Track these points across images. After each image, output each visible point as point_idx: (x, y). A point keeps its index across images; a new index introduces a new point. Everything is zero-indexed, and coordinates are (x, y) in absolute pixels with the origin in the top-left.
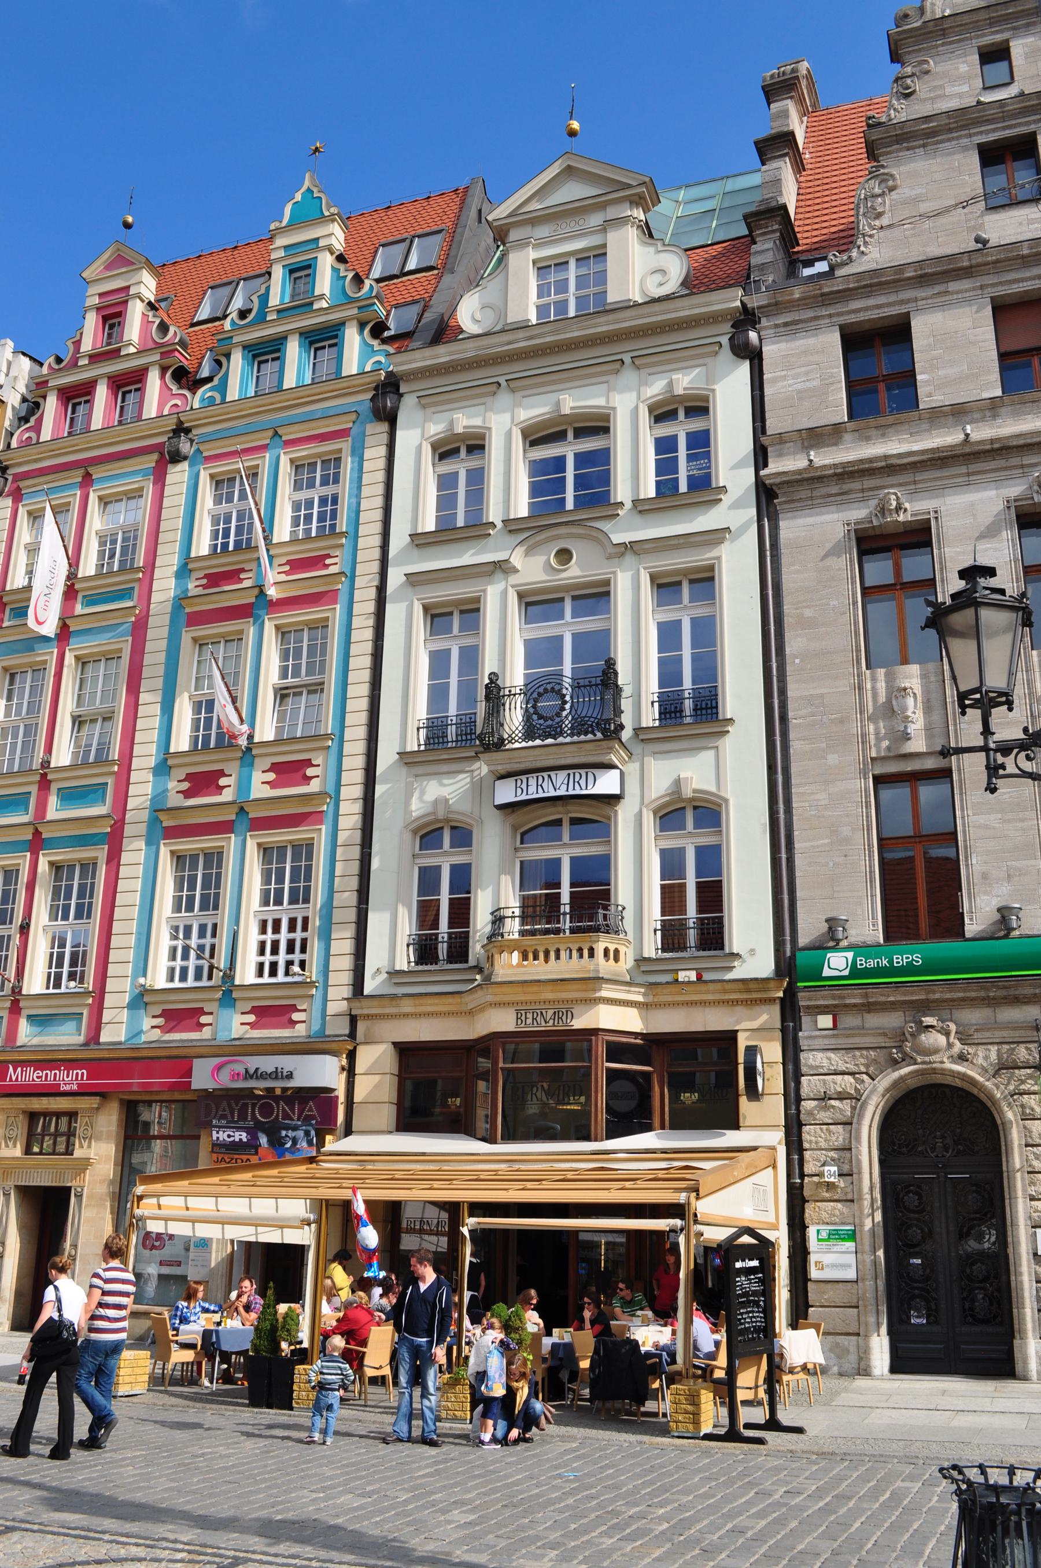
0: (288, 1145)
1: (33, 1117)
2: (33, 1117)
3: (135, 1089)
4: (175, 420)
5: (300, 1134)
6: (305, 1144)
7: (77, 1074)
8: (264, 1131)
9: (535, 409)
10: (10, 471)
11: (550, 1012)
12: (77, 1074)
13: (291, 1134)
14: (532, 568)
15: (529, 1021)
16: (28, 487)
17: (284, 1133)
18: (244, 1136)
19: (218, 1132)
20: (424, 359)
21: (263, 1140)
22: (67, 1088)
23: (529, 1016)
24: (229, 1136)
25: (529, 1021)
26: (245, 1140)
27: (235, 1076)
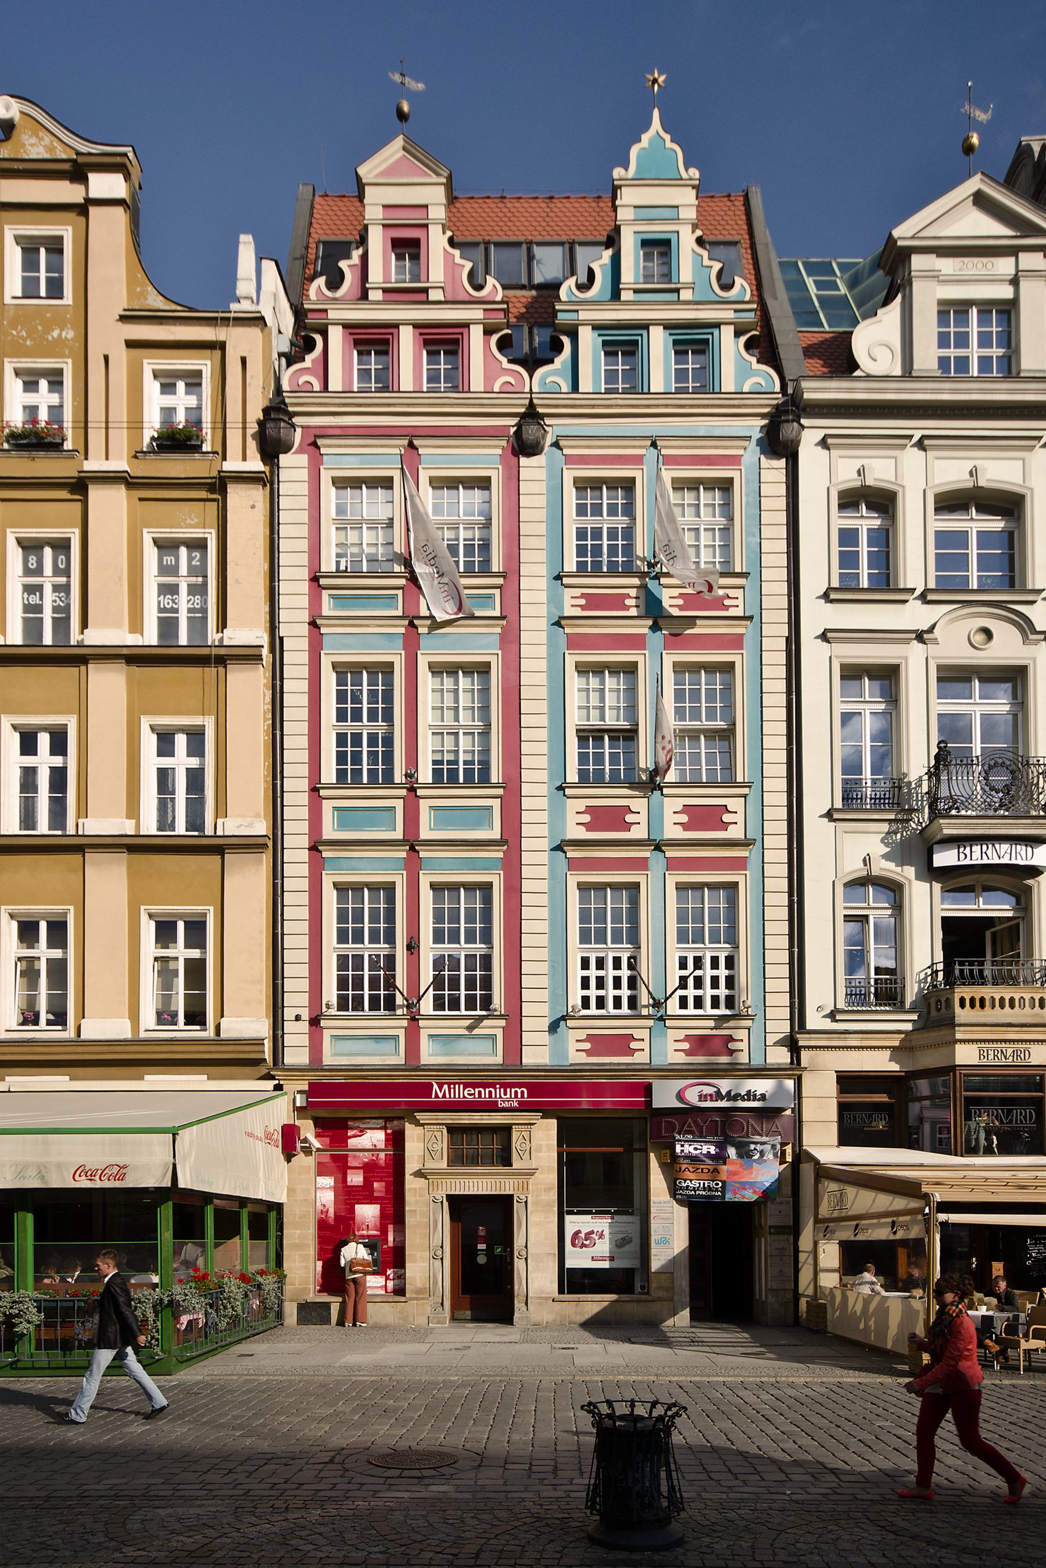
0: (756, 1157)
1: (452, 1129)
2: (452, 1129)
3: (584, 1106)
4: (527, 402)
5: (768, 1147)
6: (771, 1156)
7: (516, 1092)
8: (733, 1145)
9: (952, 471)
10: (296, 420)
11: (1010, 1051)
12: (516, 1092)
13: (759, 1147)
14: (956, 638)
15: (991, 1057)
16: (330, 446)
17: (752, 1147)
18: (713, 1150)
19: (682, 1146)
20: (839, 390)
21: (732, 1152)
22: (506, 1105)
23: (991, 1053)
24: (696, 1149)
25: (991, 1057)
26: (713, 1152)
27: (702, 1097)
